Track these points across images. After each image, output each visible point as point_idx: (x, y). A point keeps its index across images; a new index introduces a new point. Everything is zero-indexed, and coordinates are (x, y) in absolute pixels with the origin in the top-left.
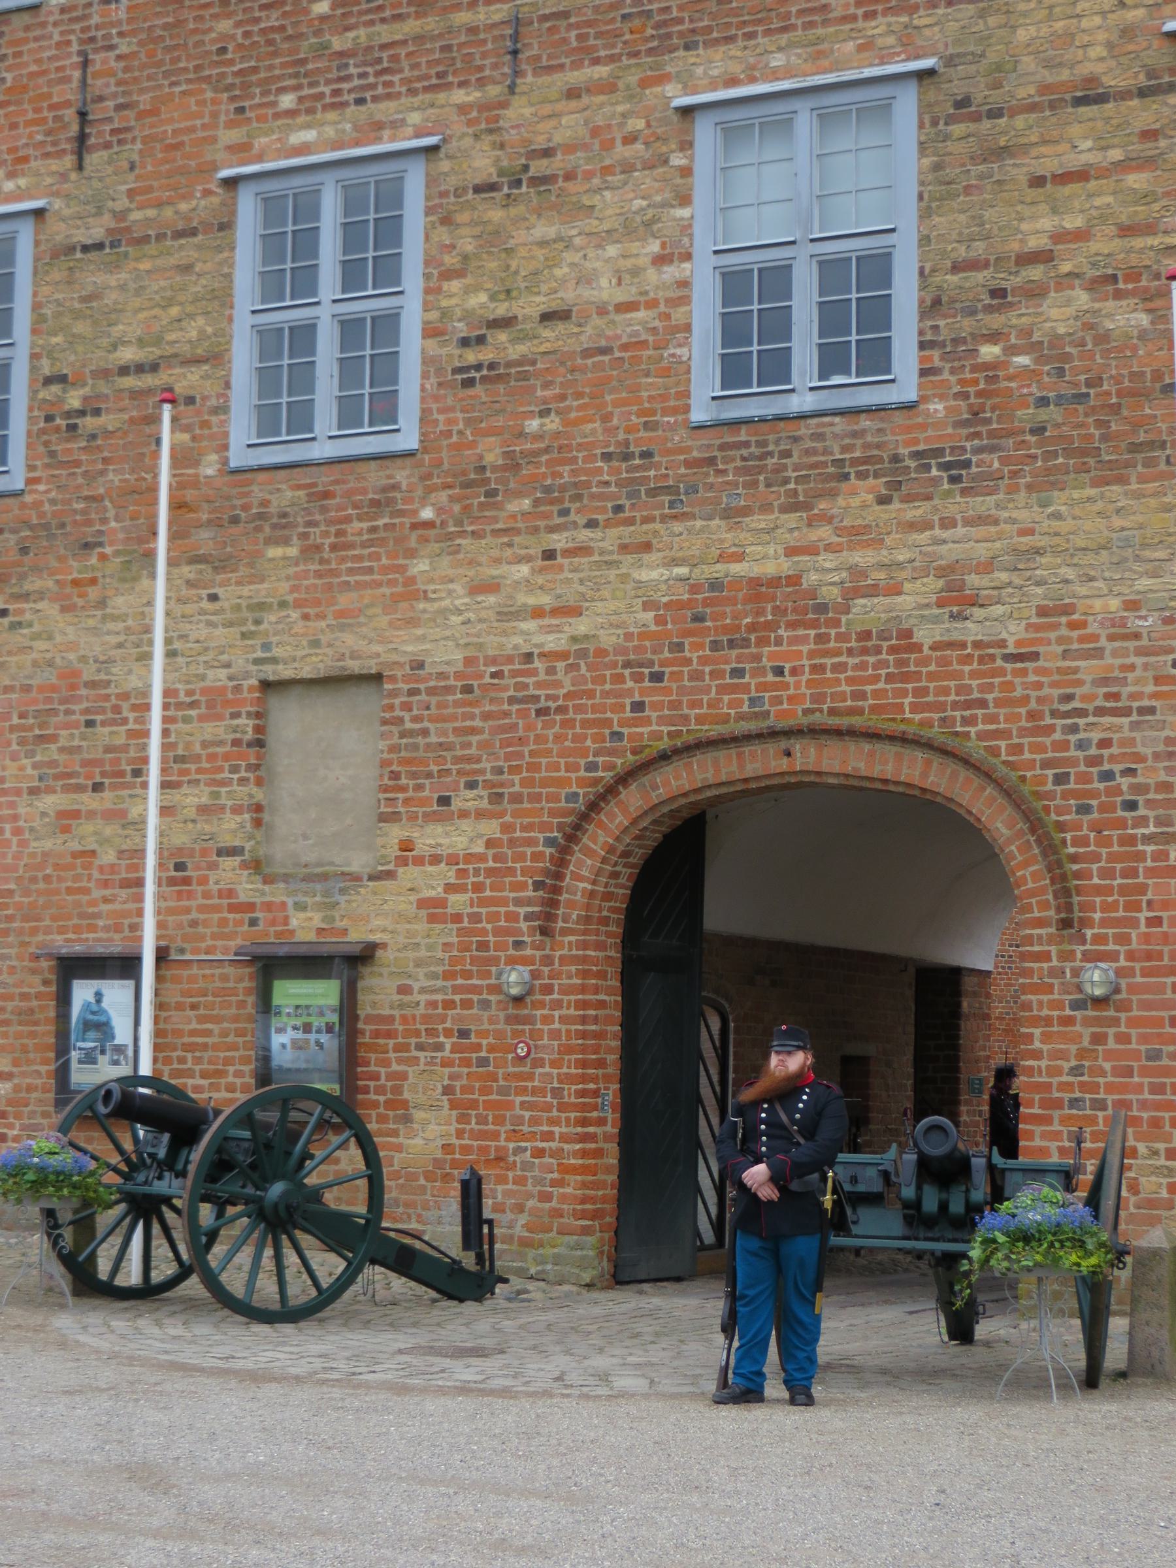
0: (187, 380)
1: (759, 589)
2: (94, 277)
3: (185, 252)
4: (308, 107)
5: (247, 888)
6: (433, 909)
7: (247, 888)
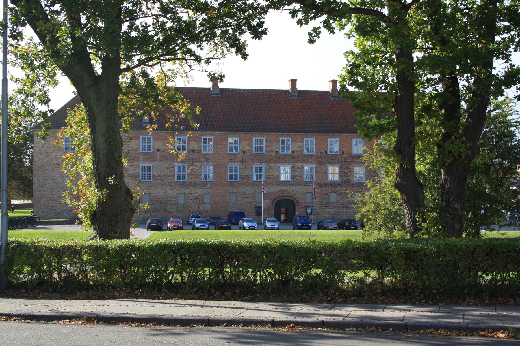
0: (250, 176)
1: (283, 190)
2: (243, 170)
3: (250, 169)
4: (257, 162)
5: (255, 204)
6: (266, 205)
7: (255, 204)
